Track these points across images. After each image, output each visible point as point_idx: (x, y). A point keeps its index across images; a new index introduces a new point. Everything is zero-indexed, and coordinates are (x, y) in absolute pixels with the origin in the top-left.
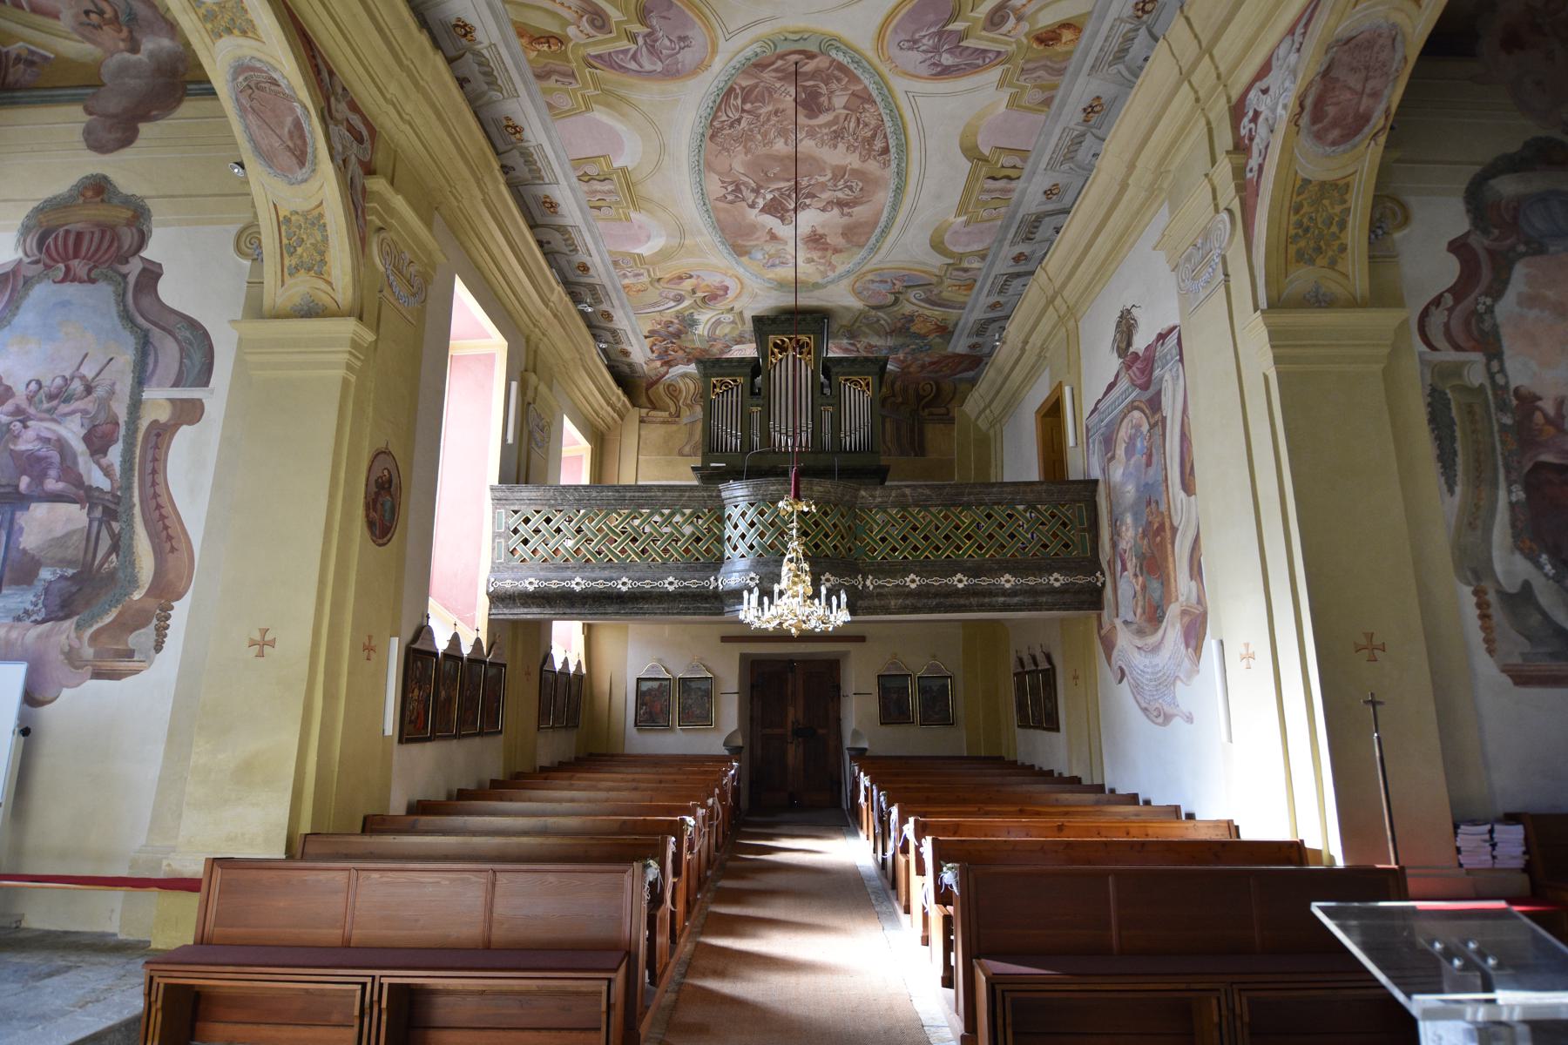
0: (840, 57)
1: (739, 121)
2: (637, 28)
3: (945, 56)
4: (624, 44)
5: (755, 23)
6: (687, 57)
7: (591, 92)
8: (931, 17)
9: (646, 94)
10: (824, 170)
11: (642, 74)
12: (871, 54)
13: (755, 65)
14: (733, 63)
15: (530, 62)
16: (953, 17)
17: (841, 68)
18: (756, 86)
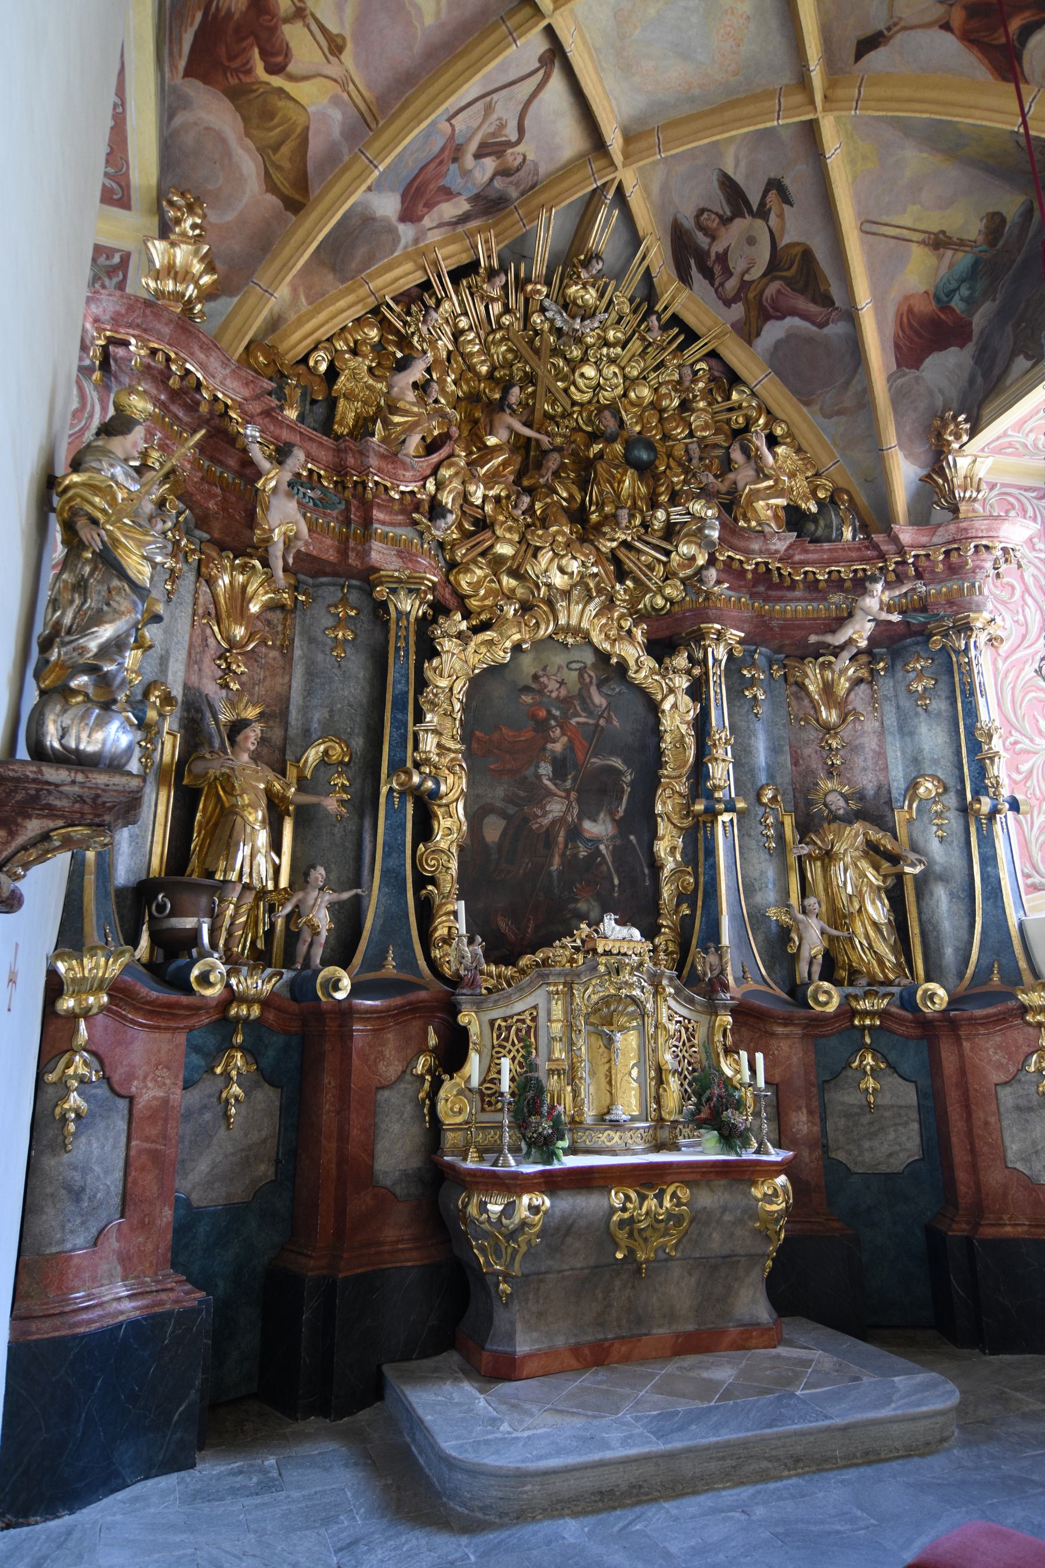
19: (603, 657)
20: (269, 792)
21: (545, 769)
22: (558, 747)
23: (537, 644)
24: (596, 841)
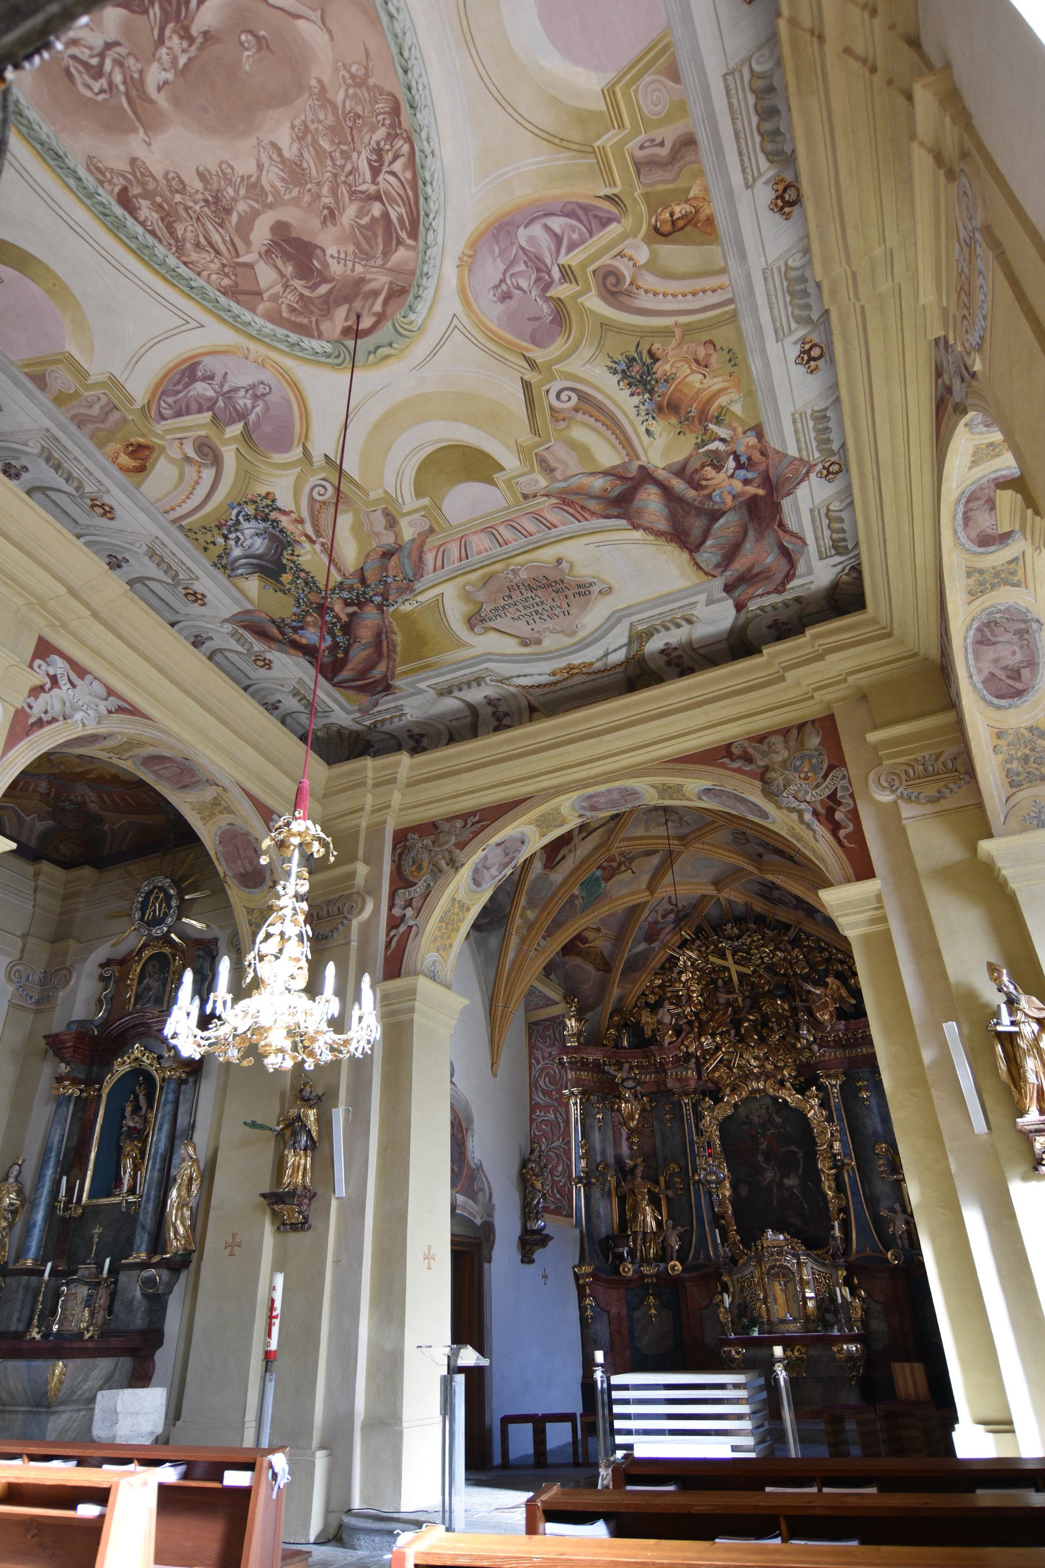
0: (316, 344)
1: (375, 172)
2: (563, 291)
3: (210, 393)
4: (572, 259)
5: (433, 353)
6: (492, 270)
7: (609, 139)
8: (267, 429)
9: (532, 172)
10: (176, 101)
11: (537, 213)
12: (288, 363)
13: (403, 291)
14: (430, 284)
15: (701, 173)
16: (247, 436)
17: (304, 330)
18: (386, 254)
19: (775, 1099)
20: (650, 1192)
21: (760, 1158)
22: (764, 1146)
23: (743, 1101)
24: (791, 1188)
